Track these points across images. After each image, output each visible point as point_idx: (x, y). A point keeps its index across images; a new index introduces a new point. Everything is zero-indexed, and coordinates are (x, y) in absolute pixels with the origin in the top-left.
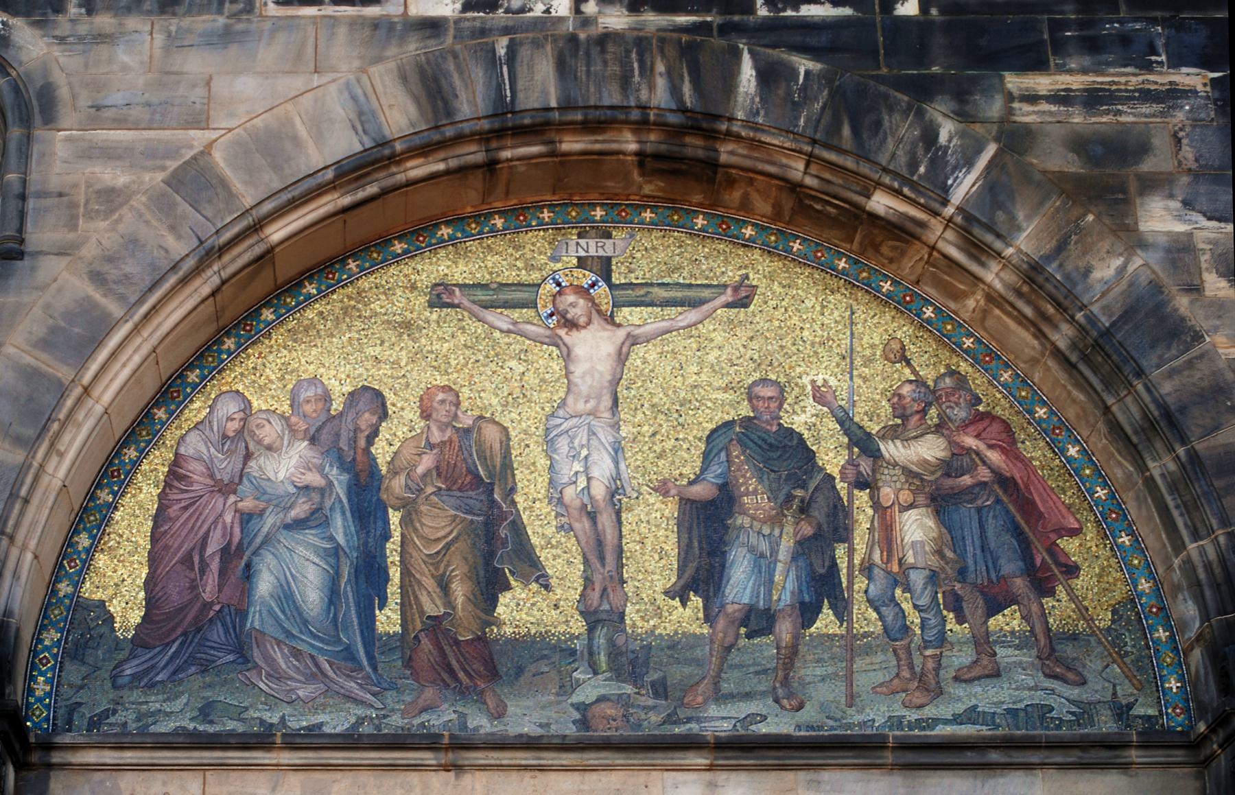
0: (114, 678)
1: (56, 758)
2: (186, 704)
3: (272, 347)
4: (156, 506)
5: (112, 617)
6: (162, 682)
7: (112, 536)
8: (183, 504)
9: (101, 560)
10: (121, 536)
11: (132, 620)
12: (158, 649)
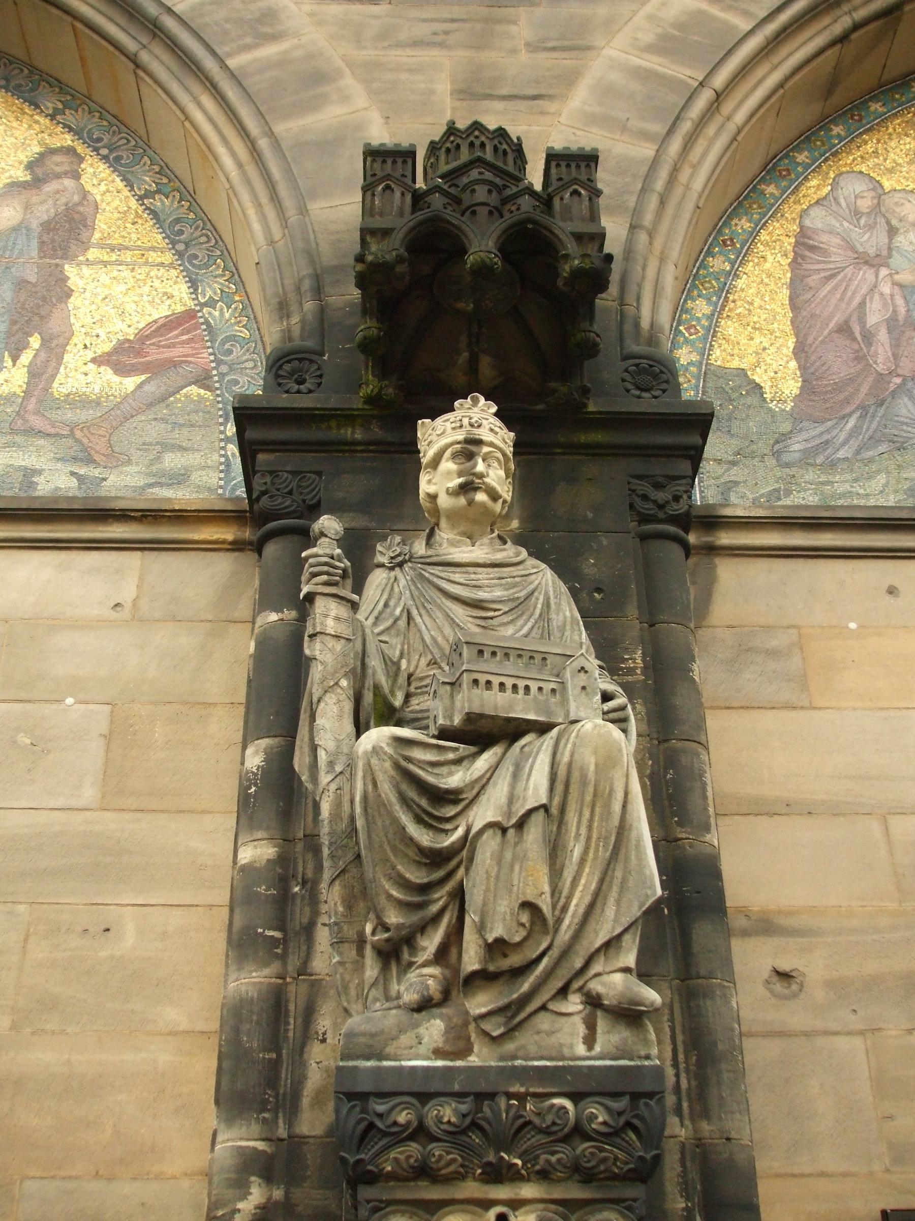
0: (777, 455)
1: (725, 538)
2: (886, 485)
3: (890, 134)
4: (789, 275)
5: (759, 387)
6: (846, 459)
7: (739, 303)
8: (823, 275)
9: (729, 327)
10: (751, 304)
11: (787, 392)
12: (830, 424)
